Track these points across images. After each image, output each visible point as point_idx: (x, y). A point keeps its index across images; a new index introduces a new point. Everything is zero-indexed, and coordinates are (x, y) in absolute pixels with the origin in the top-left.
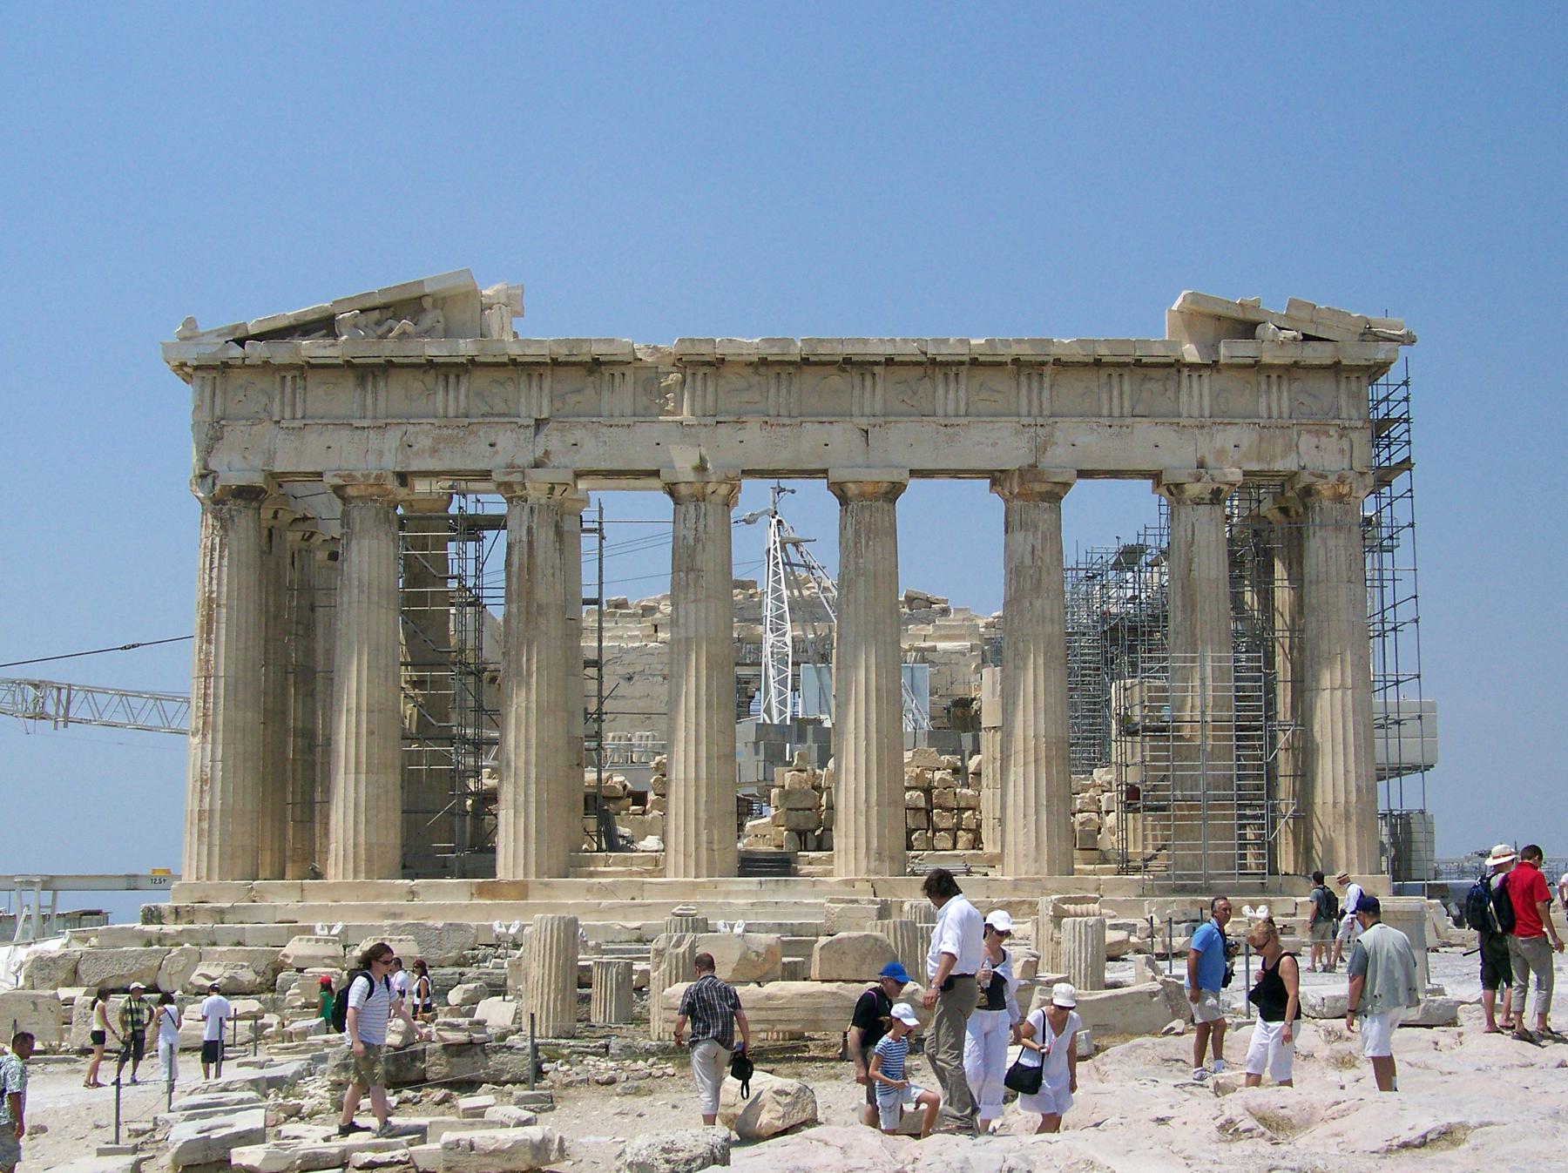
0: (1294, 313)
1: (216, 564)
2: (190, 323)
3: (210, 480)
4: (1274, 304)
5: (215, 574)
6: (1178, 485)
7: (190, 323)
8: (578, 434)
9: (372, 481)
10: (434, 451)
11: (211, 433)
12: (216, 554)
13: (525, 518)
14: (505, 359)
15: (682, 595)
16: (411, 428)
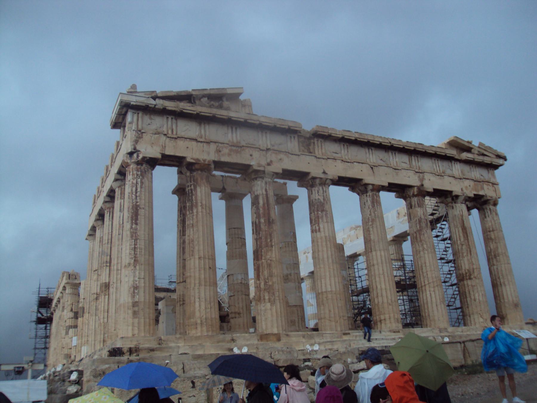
0: (481, 147)
1: (139, 190)
2: (134, 86)
3: (135, 155)
4: (476, 143)
5: (138, 194)
6: (457, 197)
7: (134, 86)
8: (282, 156)
9: (207, 163)
10: (229, 155)
11: (137, 135)
12: (139, 186)
13: (263, 185)
14: (258, 122)
15: (320, 220)
16: (220, 145)
